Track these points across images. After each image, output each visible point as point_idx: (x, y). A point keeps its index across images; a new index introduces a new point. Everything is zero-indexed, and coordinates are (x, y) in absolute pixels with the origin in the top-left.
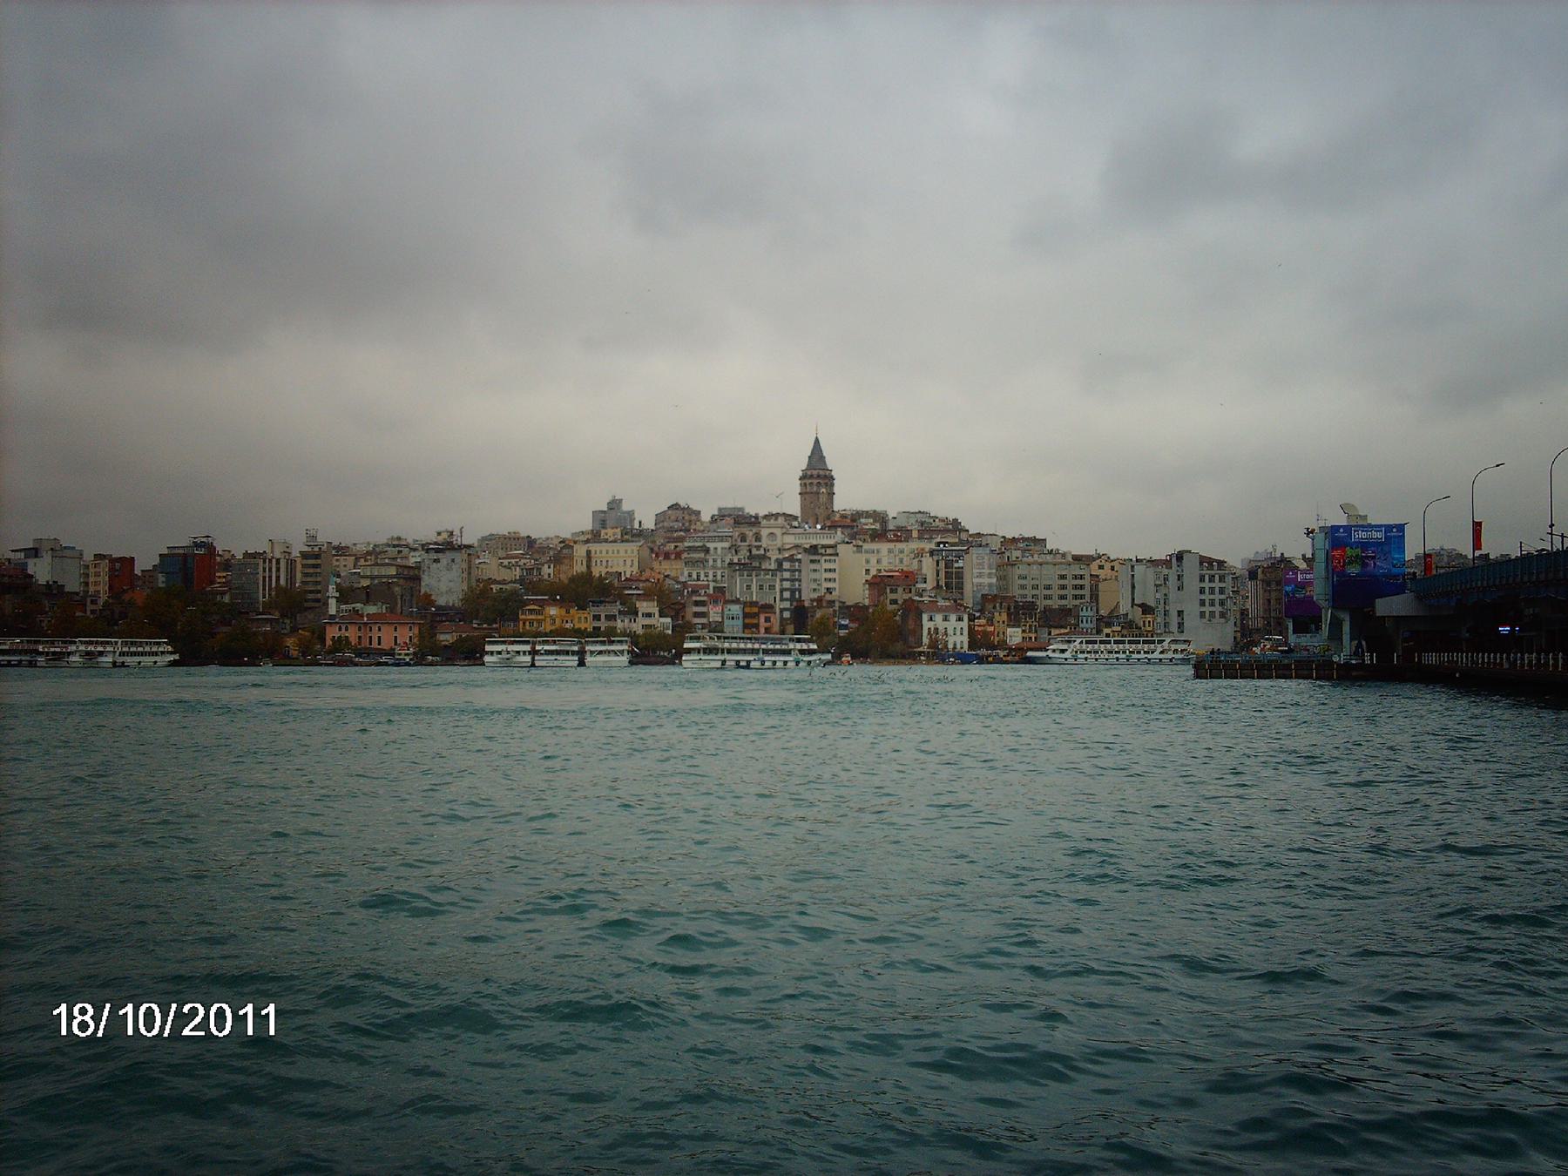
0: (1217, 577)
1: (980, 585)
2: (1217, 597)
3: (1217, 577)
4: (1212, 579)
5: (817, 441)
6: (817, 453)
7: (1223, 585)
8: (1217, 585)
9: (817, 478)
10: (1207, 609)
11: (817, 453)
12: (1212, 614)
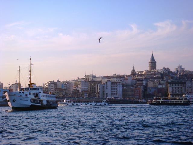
0: (115, 86)
1: (83, 89)
2: (115, 90)
3: (115, 86)
4: (114, 86)
5: (152, 55)
6: (153, 58)
7: (116, 88)
8: (115, 88)
9: (153, 63)
10: (113, 93)
11: (153, 58)
12: (114, 94)
